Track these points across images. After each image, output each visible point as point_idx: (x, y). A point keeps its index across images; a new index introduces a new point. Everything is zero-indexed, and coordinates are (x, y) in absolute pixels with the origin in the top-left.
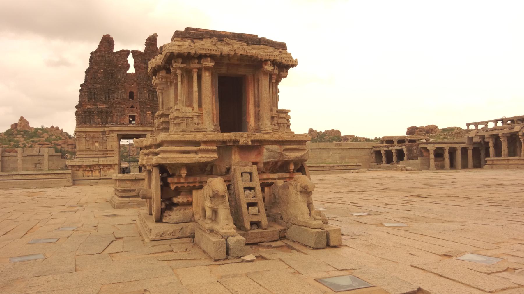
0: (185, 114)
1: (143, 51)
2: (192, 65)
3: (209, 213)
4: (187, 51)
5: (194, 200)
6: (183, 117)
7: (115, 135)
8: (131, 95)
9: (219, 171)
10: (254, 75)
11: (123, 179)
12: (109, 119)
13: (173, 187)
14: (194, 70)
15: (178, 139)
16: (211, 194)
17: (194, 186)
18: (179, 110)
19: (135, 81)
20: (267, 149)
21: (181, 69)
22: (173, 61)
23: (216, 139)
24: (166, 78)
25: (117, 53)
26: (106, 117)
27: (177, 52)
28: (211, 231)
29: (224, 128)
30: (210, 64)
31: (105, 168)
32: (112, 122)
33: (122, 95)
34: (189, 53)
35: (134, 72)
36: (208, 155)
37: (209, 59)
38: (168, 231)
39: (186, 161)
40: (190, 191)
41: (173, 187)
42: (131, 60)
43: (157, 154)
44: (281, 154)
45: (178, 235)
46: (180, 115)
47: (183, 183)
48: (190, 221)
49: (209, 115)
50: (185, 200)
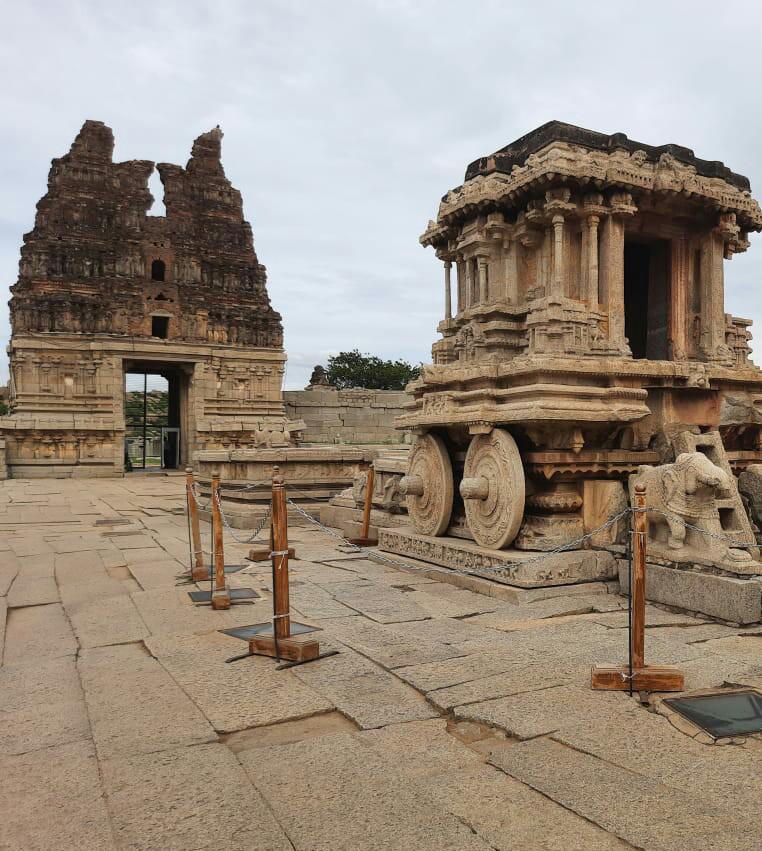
0: (573, 314)
3: (678, 528)
4: (588, 174)
5: (586, 503)
6: (568, 322)
7: (116, 361)
9: (636, 443)
12: (102, 323)
13: (549, 473)
15: (571, 369)
16: (692, 486)
17: (589, 472)
18: (559, 305)
19: (166, 236)
21: (563, 212)
22: (548, 194)
23: (645, 372)
24: (501, 231)
25: (121, 165)
26: (91, 315)
28: (686, 565)
29: (639, 352)
30: (632, 209)
31: (92, 440)
32: (106, 330)
33: (132, 266)
34: (593, 178)
35: (164, 215)
36: (634, 406)
37: (630, 197)
39: (588, 416)
40: (576, 483)
41: (549, 473)
42: (155, 185)
43: (500, 400)
45: (577, 576)
46: (564, 317)
47: (569, 465)
50: (570, 502)
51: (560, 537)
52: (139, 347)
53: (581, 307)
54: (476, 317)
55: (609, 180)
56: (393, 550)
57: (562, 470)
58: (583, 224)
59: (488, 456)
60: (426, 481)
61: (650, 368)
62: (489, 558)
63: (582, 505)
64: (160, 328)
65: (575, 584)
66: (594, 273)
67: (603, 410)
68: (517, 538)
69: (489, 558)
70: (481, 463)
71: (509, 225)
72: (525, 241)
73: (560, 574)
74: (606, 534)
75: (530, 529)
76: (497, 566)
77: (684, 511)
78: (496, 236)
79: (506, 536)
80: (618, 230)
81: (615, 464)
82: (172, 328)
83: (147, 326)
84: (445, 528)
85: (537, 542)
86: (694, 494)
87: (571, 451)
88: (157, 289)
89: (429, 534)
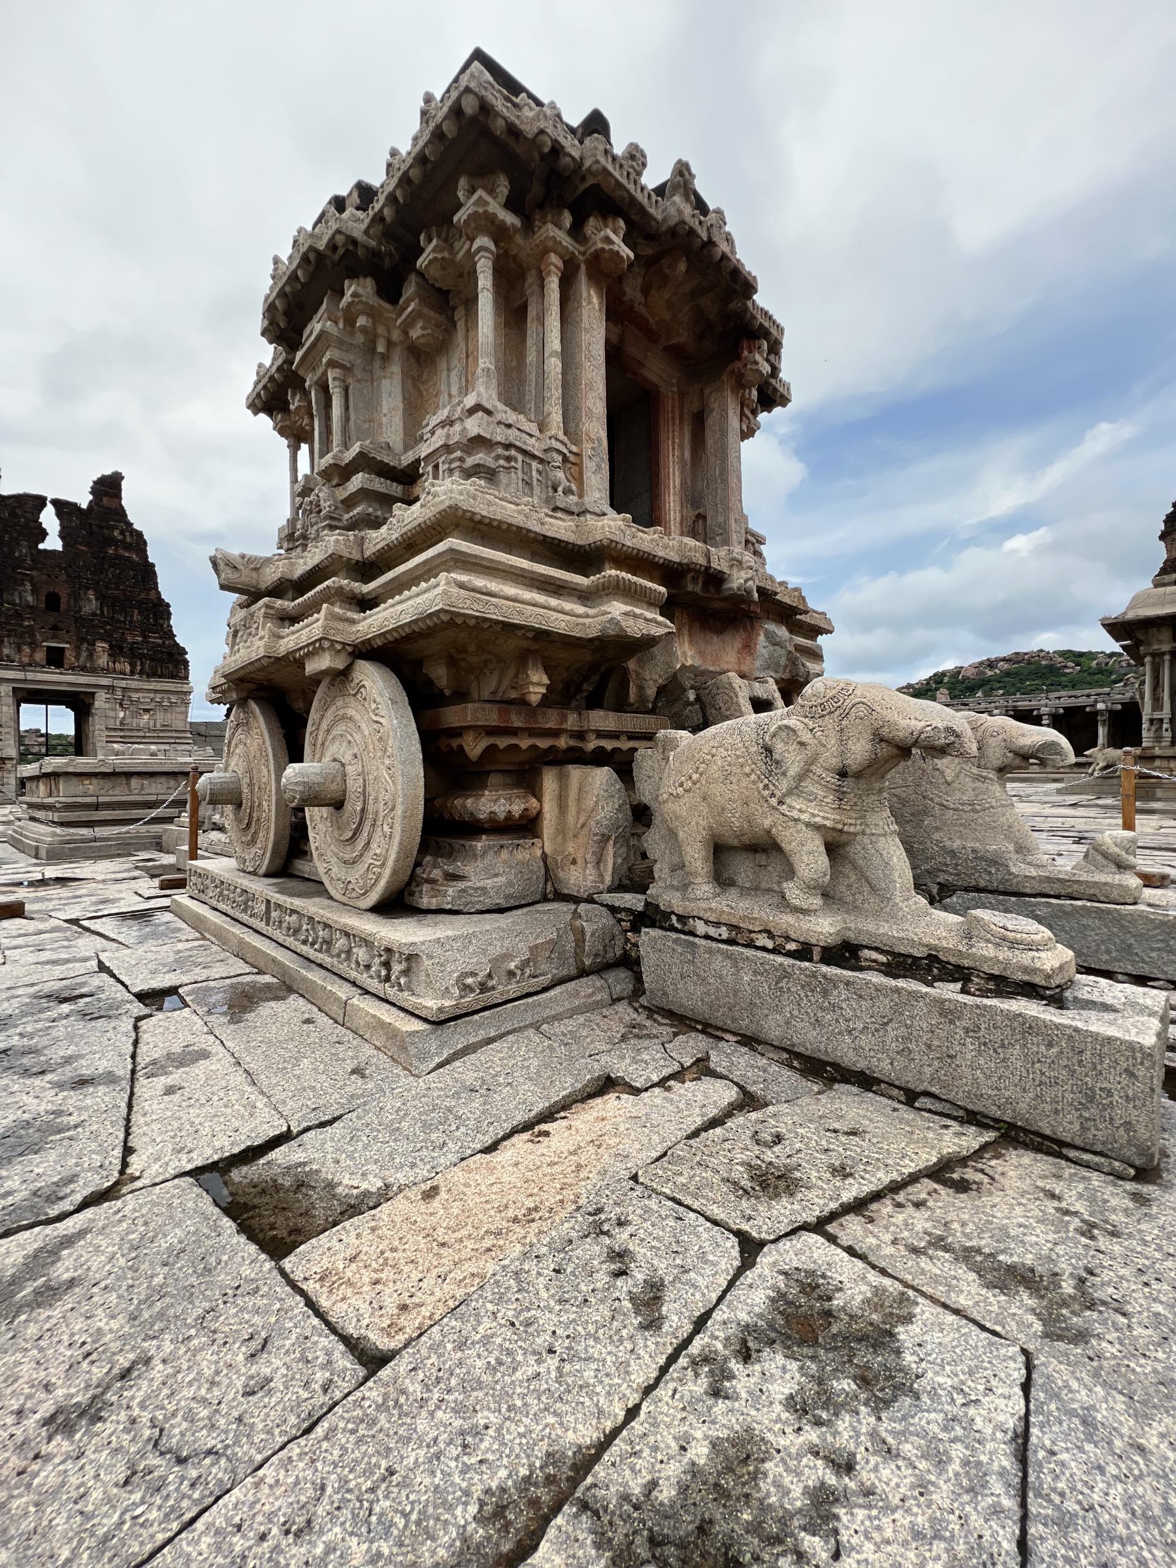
1: (84, 506)
2: (551, 230)
3: (811, 859)
5: (547, 808)
6: (508, 446)
8: (53, 602)
10: (682, 395)
11: (70, 770)
13: (474, 747)
14: (554, 258)
18: (489, 413)
19: (61, 569)
20: (769, 636)
21: (500, 233)
22: (463, 183)
27: (506, 114)
37: (621, 223)
38: (507, 956)
41: (474, 747)
43: (366, 604)
44: (793, 662)
46: (500, 435)
48: (545, 899)
49: (599, 467)
50: (517, 808)
51: (501, 880)
52: (30, 676)
53: (533, 428)
54: (327, 474)
55: (587, 163)
56: (203, 897)
57: (503, 742)
58: (531, 279)
59: (344, 718)
60: (245, 781)
61: (665, 547)
62: (347, 935)
63: (540, 813)
64: (55, 659)
65: (545, 990)
66: (554, 365)
67: (587, 616)
68: (409, 884)
69: (347, 935)
70: (334, 732)
71: (387, 306)
72: (416, 333)
73: (511, 974)
74: (591, 871)
75: (435, 866)
76: (361, 953)
77: (826, 816)
78: (362, 321)
79: (382, 883)
80: (595, 300)
81: (600, 734)
82: (69, 656)
83: (40, 656)
84: (279, 862)
85: (450, 894)
86: (858, 775)
87: (522, 702)
88: (52, 619)
89: (254, 873)
